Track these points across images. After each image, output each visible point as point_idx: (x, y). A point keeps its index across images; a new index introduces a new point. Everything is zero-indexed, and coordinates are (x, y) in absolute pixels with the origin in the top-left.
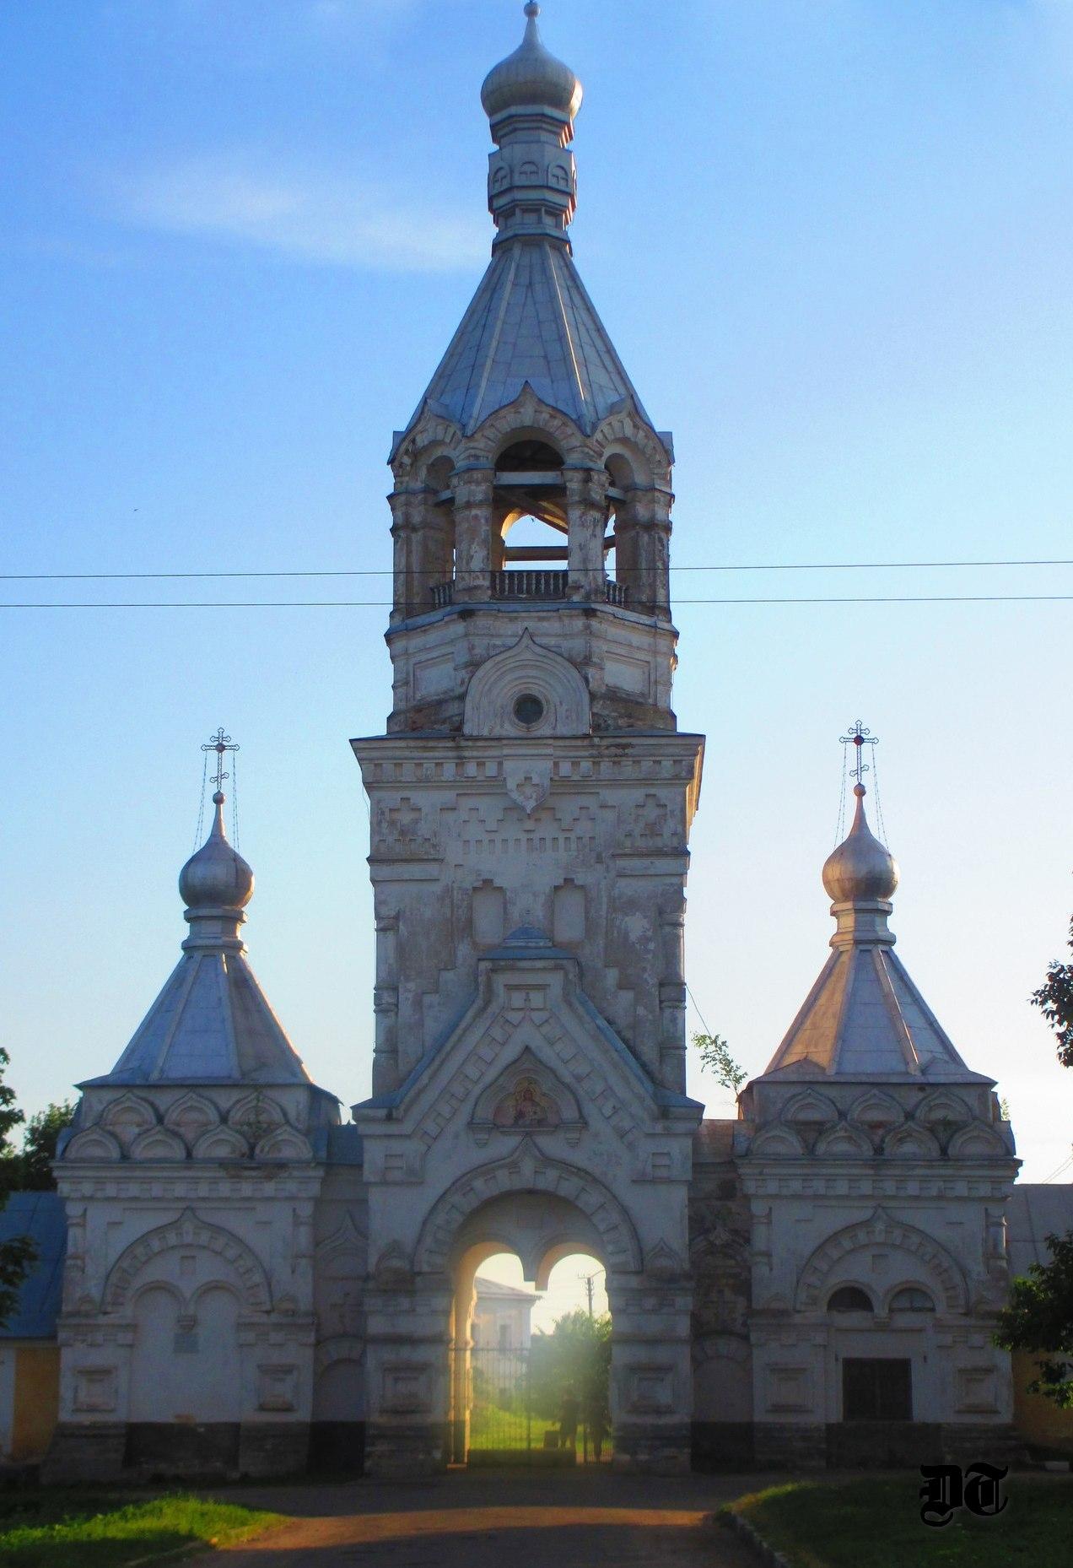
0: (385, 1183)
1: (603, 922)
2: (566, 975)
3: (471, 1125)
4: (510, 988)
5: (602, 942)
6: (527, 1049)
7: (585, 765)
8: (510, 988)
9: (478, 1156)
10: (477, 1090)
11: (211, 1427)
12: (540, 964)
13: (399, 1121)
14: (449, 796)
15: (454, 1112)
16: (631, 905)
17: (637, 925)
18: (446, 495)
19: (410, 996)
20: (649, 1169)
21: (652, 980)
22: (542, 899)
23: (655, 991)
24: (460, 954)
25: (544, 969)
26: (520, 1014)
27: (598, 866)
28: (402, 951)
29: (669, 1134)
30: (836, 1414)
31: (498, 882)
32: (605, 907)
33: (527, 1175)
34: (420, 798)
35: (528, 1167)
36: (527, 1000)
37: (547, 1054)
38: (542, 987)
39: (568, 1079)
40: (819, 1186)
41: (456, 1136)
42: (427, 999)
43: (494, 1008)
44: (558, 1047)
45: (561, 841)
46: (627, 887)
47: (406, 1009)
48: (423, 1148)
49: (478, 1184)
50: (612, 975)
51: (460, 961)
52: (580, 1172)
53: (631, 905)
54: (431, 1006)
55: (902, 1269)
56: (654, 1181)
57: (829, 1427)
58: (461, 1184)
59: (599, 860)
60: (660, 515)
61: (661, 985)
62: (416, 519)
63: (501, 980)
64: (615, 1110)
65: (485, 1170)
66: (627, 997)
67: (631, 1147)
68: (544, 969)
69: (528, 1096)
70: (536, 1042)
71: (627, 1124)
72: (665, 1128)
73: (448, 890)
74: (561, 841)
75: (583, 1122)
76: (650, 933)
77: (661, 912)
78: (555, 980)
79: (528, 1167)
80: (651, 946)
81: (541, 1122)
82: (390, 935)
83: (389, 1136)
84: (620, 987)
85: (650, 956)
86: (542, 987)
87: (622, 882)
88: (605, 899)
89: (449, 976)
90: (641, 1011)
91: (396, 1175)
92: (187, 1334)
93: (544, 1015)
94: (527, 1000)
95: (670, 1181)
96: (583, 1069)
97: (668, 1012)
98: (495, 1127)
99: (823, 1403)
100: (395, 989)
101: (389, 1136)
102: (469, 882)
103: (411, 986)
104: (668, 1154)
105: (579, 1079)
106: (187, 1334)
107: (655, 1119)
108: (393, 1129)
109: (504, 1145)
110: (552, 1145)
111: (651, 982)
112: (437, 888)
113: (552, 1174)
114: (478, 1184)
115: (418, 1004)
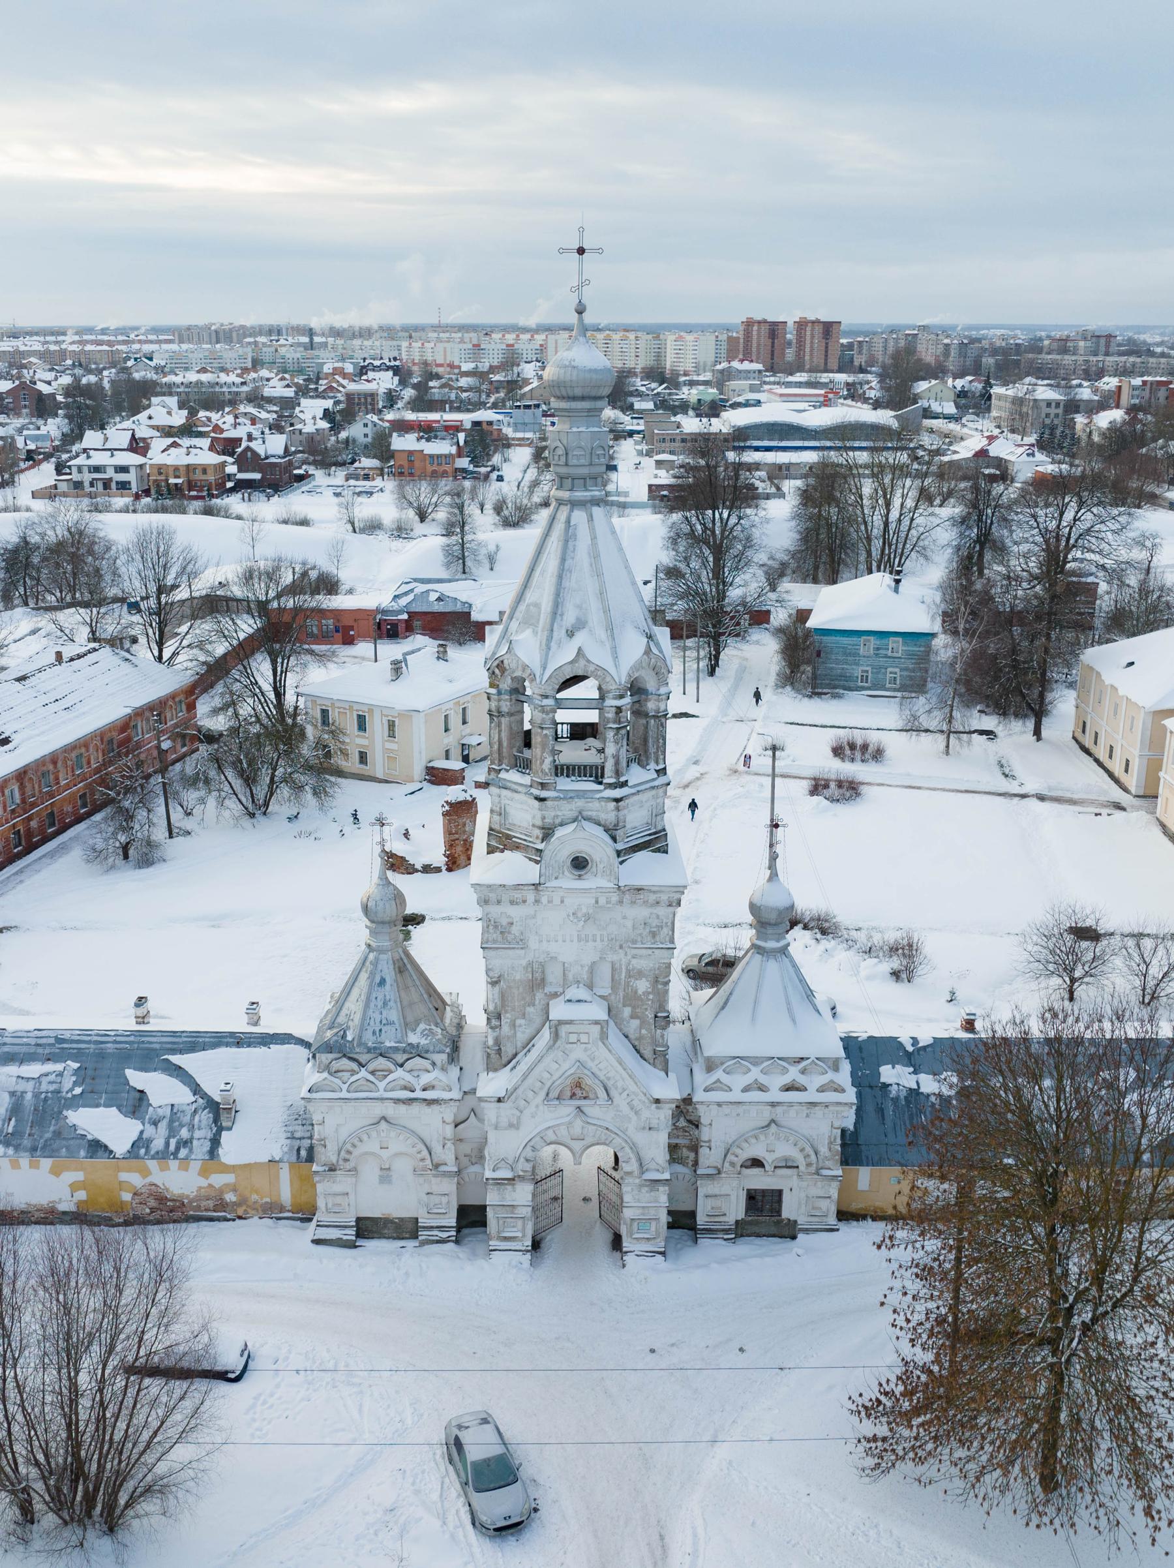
11: (401, 1219)
17: (642, 986)
21: (650, 1015)
23: (652, 1021)
28: (503, 996)
30: (741, 1215)
41: (537, 1106)
46: (638, 964)
50: (627, 1011)
53: (640, 974)
55: (785, 1150)
57: (737, 1222)
59: (621, 947)
60: (662, 708)
62: (505, 709)
66: (635, 1023)
67: (636, 1113)
73: (530, 964)
80: (651, 997)
84: (632, 1017)
87: (634, 961)
88: (624, 970)
89: (530, 1010)
90: (644, 1031)
92: (386, 1175)
99: (736, 1210)
106: (386, 1175)
112: (524, 962)
115: (513, 1025)
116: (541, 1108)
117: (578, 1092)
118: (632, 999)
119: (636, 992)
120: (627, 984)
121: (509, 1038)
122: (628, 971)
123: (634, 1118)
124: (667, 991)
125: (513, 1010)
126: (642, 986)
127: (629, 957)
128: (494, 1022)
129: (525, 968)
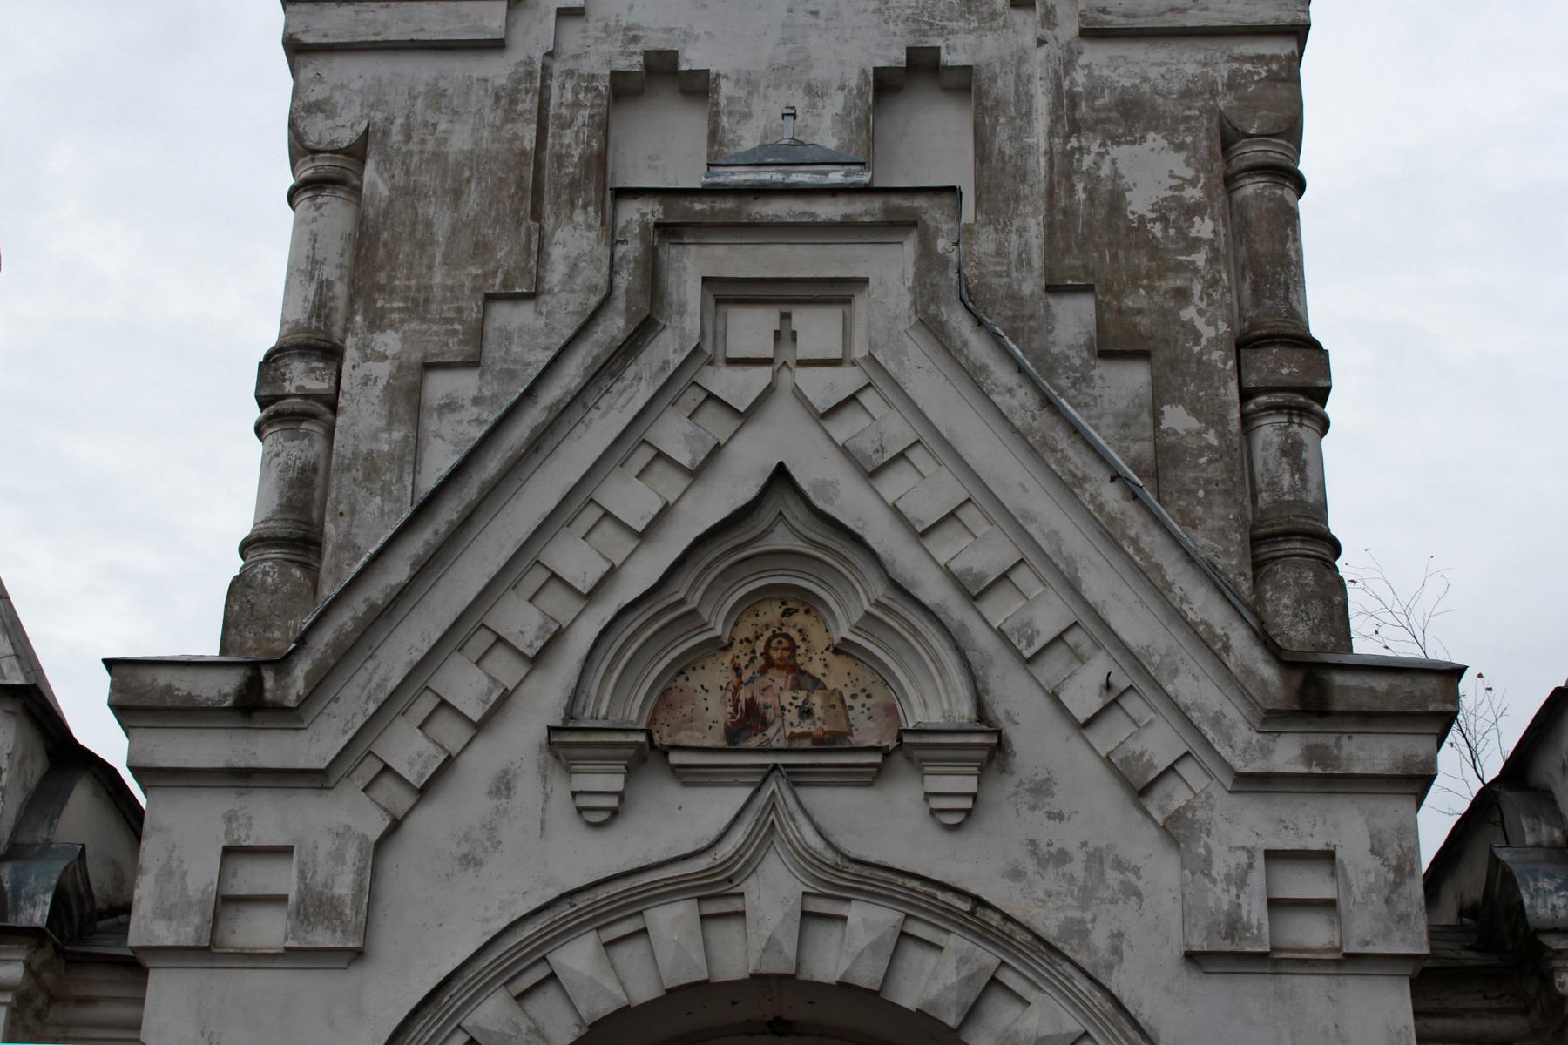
0: (206, 953)
1: (1039, 165)
2: (926, 250)
3: (567, 743)
4: (726, 293)
5: (1034, 228)
6: (781, 475)
8: (726, 293)
9: (587, 858)
12: (827, 210)
13: (290, 716)
15: (502, 703)
16: (1133, 115)
17: (1151, 172)
19: (382, 370)
20: (1255, 911)
21: (1207, 325)
22: (836, 103)
24: (556, 253)
25: (846, 228)
26: (760, 377)
27: (1018, 16)
28: (364, 244)
29: (1331, 782)
31: (692, 59)
32: (1041, 124)
33: (763, 930)
35: (773, 893)
36: (784, 336)
37: (852, 502)
38: (837, 292)
39: (934, 591)
41: (503, 786)
42: (439, 386)
43: (666, 349)
44: (895, 485)
47: (364, 418)
48: (375, 826)
49: (578, 958)
50: (1073, 320)
51: (555, 275)
52: (975, 915)
53: (1133, 115)
54: (450, 406)
56: (1269, 962)
58: (516, 958)
61: (1245, 343)
63: (690, 268)
64: (1113, 704)
65: (612, 907)
67: (1177, 832)
68: (846, 228)
69: (783, 657)
70: (817, 469)
71: (1159, 744)
72: (1311, 754)
75: (989, 748)
76: (1193, 194)
77: (1229, 136)
78: (889, 269)
79: (773, 893)
80: (1203, 228)
81: (827, 743)
82: (336, 212)
83: (243, 777)
85: (1200, 258)
86: (837, 292)
87: (1096, 55)
88: (1042, 102)
90: (1177, 418)
93: (846, 380)
94: (784, 336)
95: (1350, 962)
96: (984, 552)
97: (1269, 431)
98: (648, 755)
100: (331, 354)
101: (243, 777)
102: (598, 54)
103: (389, 341)
104: (1327, 857)
105: (974, 592)
107: (1273, 720)
108: (268, 748)
109: (684, 820)
111: (1208, 332)
113: (868, 921)
114: (578, 958)
115: (408, 397)
116: (528, 788)
117: (778, 693)
118: (1094, 248)
119: (1116, 203)
120: (1064, 168)
121: (372, 467)
122: (1066, 107)
123: (1162, 871)
124: (1292, 217)
125: (418, 307)
126: (1151, 172)
127: (1069, 29)
128: (302, 377)
129: (507, 99)
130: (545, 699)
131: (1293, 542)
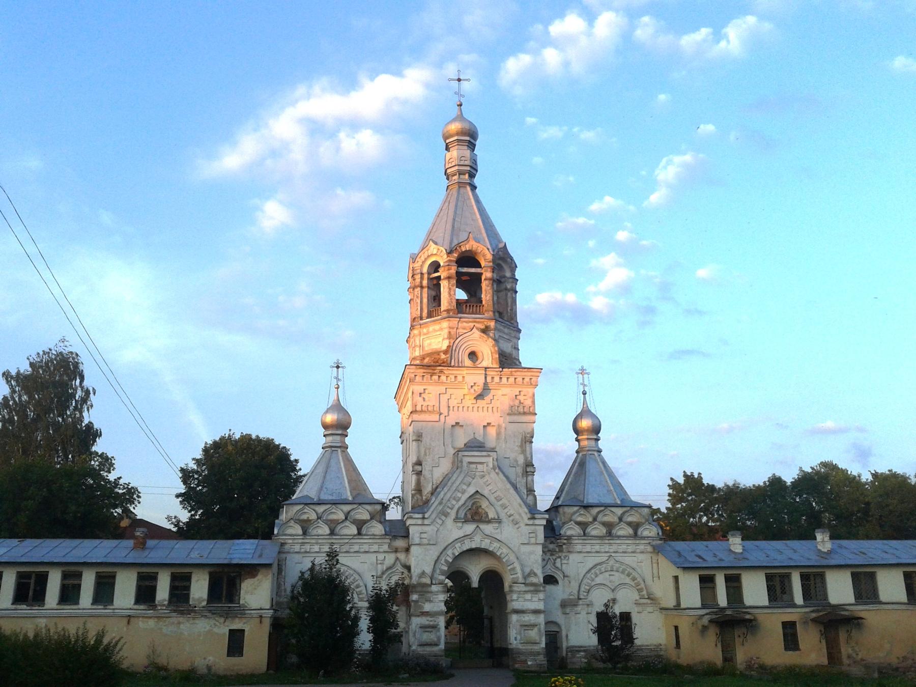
3: (456, 519)
7: (497, 379)
9: (460, 533)
10: (457, 507)
14: (442, 389)
18: (436, 275)
34: (430, 388)
40: (588, 548)
45: (485, 409)
74: (485, 409)
91: (425, 541)
98: (466, 521)
109: (470, 528)
110: (488, 528)
130: (453, 514)
131: (531, 491)
